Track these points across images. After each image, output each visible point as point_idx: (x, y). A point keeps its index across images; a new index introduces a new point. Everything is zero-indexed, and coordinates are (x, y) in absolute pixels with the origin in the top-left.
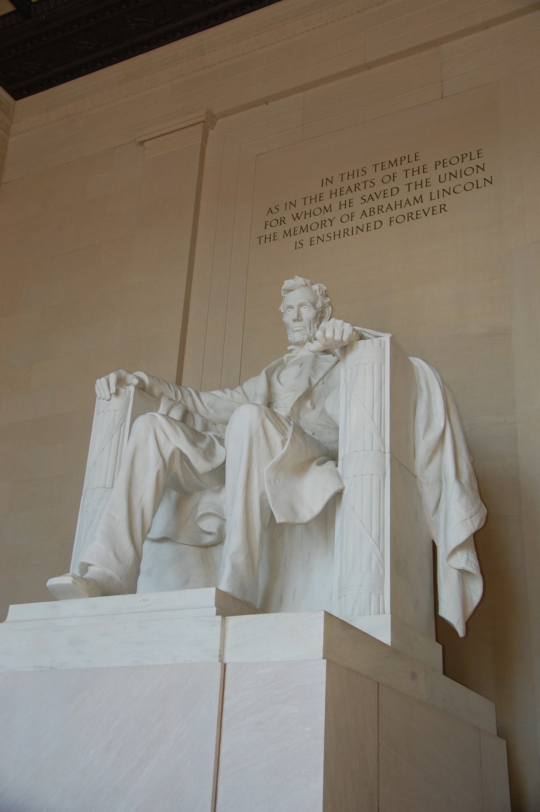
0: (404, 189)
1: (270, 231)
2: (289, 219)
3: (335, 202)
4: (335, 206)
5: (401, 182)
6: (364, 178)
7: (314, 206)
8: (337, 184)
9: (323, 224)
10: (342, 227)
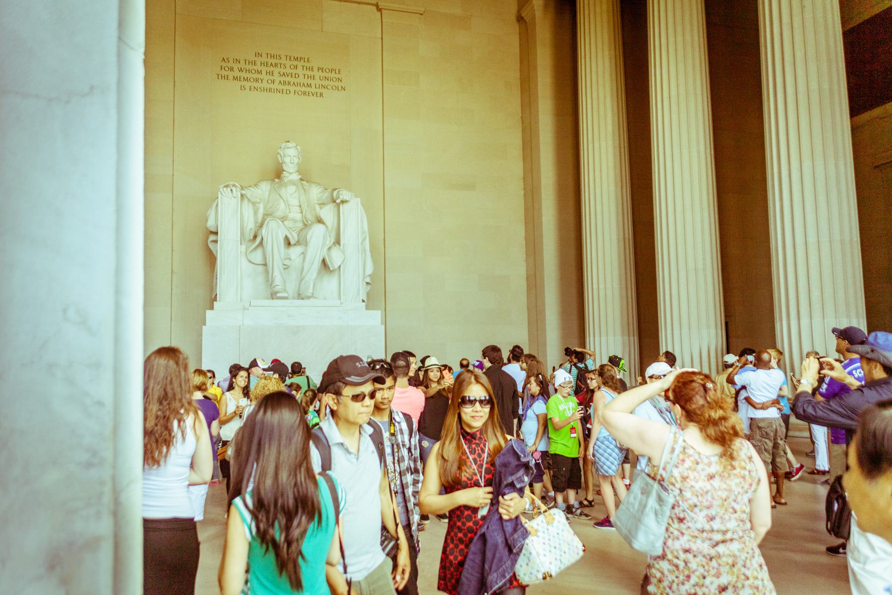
0: (302, 76)
1: (224, 73)
2: (236, 69)
3: (264, 69)
4: (264, 72)
5: (299, 71)
6: (280, 61)
7: (250, 67)
8: (264, 59)
9: (257, 80)
10: (269, 86)
